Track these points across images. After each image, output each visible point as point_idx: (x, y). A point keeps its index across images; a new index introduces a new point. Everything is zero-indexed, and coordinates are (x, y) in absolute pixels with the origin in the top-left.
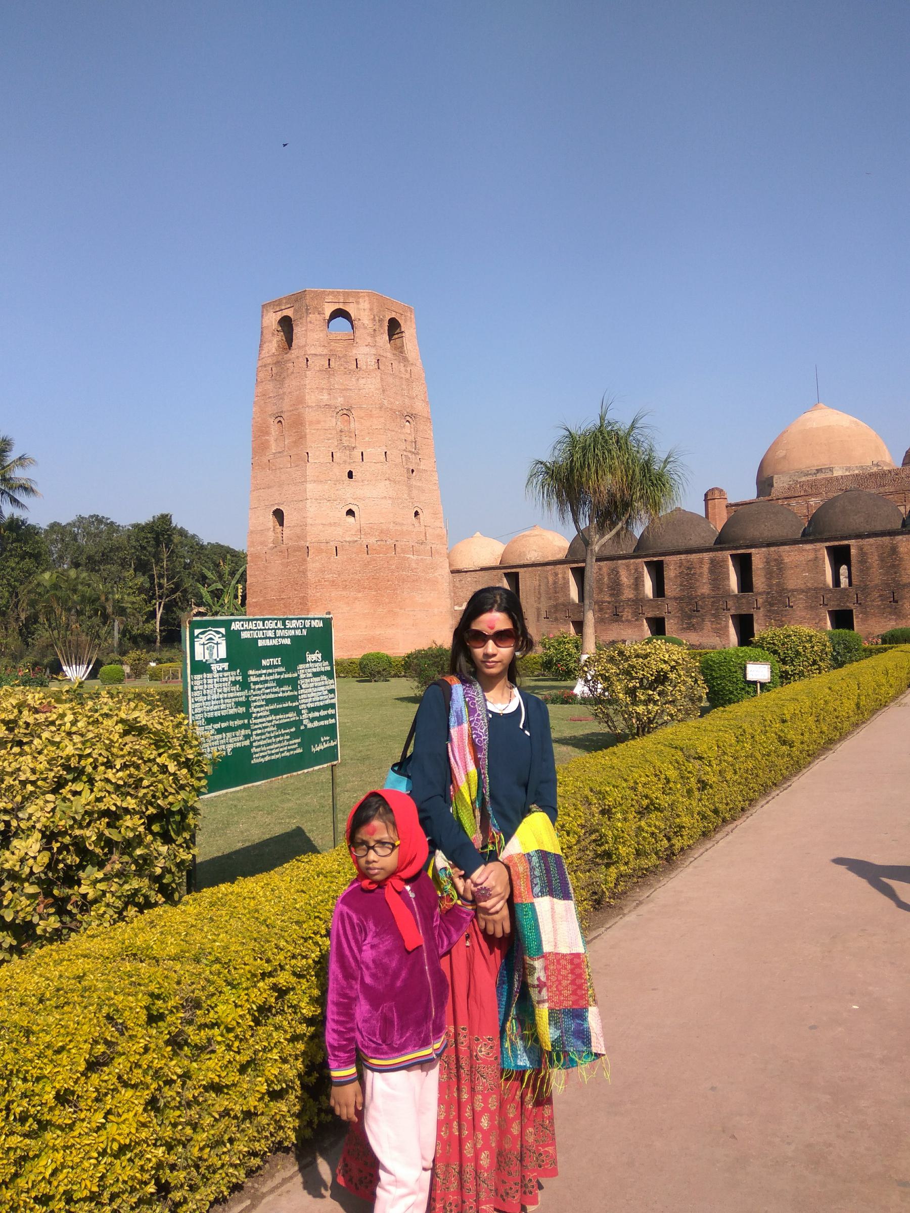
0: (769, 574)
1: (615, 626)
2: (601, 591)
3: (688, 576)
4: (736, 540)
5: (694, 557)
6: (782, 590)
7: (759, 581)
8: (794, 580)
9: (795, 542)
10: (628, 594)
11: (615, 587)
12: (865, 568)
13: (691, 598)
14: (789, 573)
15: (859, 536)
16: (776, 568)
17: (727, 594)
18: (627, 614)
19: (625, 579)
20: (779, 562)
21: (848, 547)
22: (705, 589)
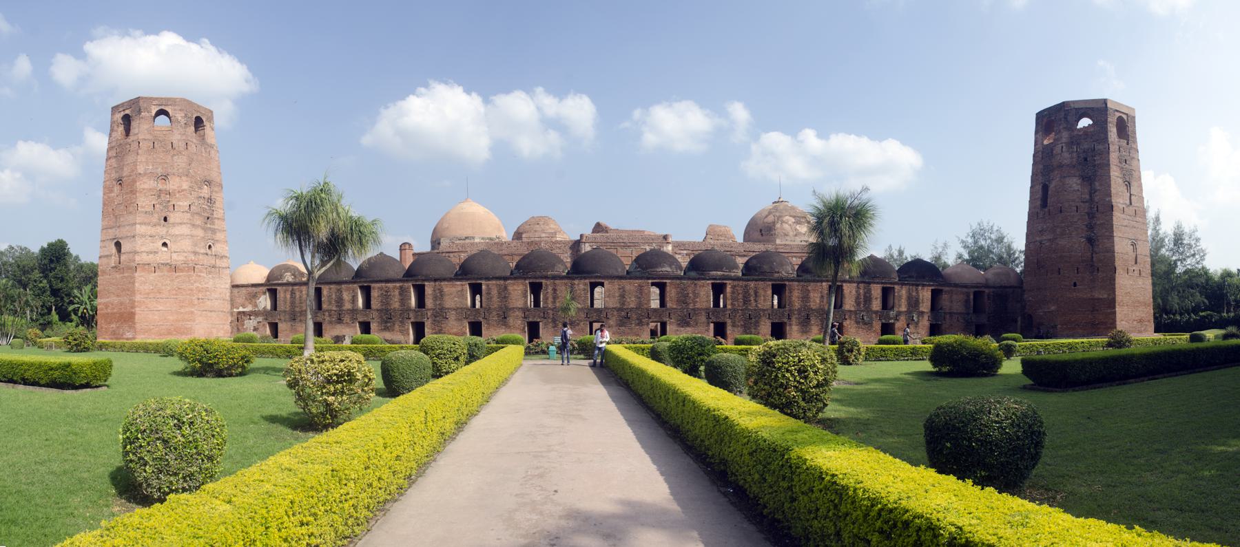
0: (435, 298)
1: (338, 326)
2: (330, 303)
3: (386, 296)
4: (418, 274)
5: (390, 285)
6: (442, 309)
7: (429, 302)
8: (449, 303)
9: (451, 279)
10: (348, 306)
11: (340, 301)
12: (490, 299)
13: (387, 310)
14: (446, 298)
15: (487, 279)
16: (439, 295)
17: (409, 309)
18: (347, 319)
19: (346, 296)
20: (441, 291)
21: (481, 285)
22: (396, 304)
